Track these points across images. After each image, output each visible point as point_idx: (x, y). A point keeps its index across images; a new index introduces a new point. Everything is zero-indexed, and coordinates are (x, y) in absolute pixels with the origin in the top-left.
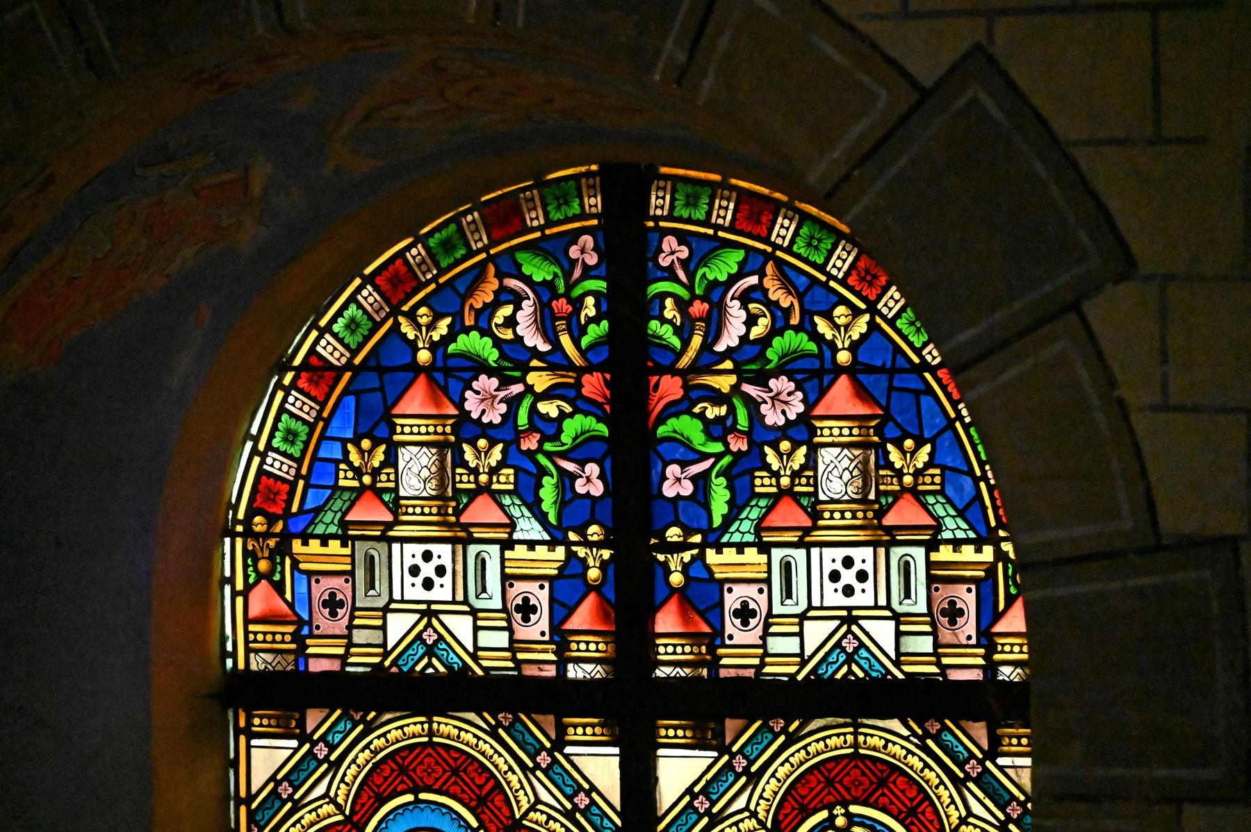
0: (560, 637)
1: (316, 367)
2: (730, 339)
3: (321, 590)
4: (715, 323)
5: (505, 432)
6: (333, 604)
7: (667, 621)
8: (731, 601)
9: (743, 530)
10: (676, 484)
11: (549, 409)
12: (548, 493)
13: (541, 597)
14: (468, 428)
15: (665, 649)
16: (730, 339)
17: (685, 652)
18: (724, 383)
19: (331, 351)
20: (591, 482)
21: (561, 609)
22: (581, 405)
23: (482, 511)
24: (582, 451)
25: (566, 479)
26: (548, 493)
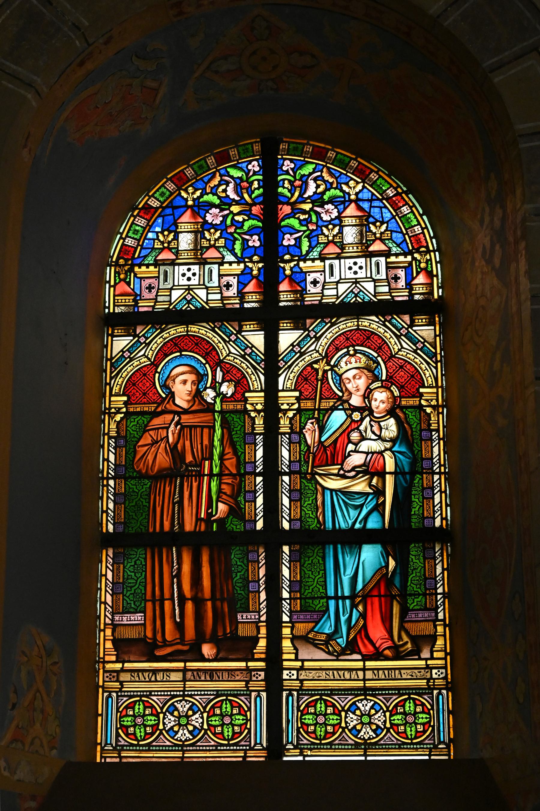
0: (241, 295)
1: (147, 208)
2: (310, 192)
3: (145, 283)
4: (304, 186)
5: (222, 227)
6: (150, 288)
7: (284, 286)
8: (310, 279)
9: (315, 254)
10: (288, 240)
11: (239, 218)
12: (238, 247)
13: (234, 281)
14: (206, 226)
15: (283, 296)
16: (310, 192)
17: (291, 297)
18: (307, 207)
19: (155, 203)
20: (255, 241)
21: (242, 285)
22: (251, 216)
23: (212, 254)
24: (251, 232)
25: (245, 242)
26: (238, 247)
